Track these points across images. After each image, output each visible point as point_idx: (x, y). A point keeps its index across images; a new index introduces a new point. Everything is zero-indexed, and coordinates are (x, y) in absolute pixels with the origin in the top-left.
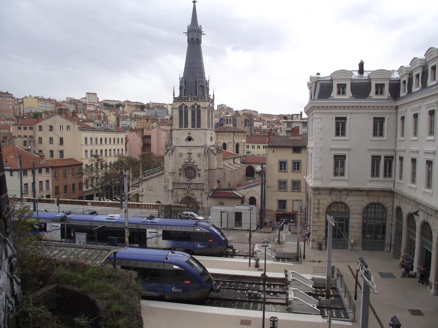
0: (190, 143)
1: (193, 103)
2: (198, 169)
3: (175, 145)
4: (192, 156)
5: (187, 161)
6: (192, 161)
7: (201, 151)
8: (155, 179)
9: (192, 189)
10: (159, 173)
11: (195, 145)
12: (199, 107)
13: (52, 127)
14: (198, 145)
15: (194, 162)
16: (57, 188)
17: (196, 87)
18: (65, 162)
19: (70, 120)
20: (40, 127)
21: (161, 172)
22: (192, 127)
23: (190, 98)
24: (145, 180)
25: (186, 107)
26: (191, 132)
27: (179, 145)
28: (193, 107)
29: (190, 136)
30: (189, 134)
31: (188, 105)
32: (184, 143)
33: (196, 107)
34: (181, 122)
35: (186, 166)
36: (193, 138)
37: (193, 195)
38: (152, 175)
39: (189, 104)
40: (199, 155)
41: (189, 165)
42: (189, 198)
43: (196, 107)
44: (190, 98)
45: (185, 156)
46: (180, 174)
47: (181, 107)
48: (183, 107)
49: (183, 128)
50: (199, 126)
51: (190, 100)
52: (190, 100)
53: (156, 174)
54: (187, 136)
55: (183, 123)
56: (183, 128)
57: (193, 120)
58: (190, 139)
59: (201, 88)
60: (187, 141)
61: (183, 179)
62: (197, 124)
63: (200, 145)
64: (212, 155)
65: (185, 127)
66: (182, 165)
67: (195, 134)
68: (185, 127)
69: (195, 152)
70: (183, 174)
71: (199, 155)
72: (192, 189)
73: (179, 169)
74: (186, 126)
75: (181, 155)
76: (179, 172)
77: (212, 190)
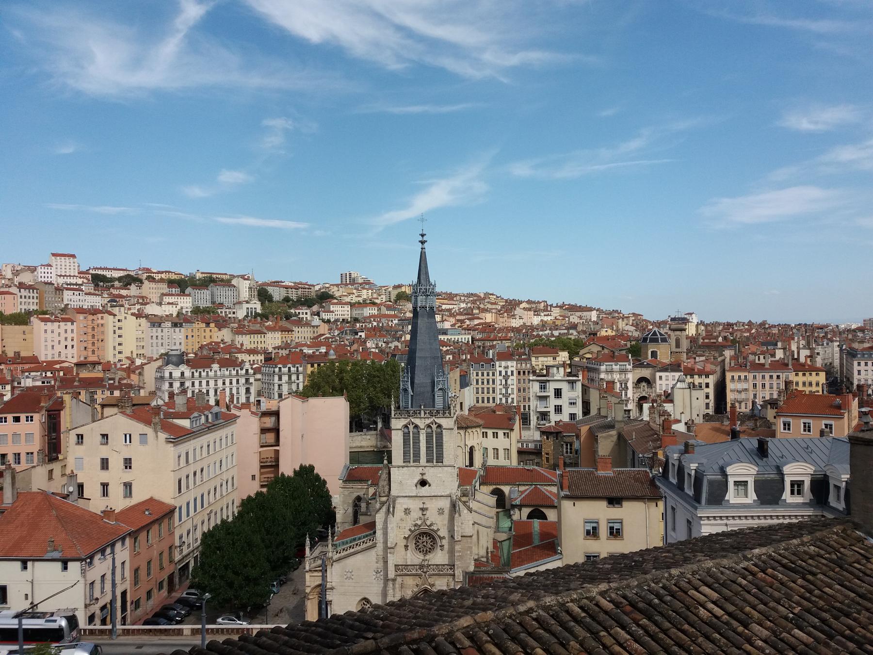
0: (425, 491)
1: (428, 421)
2: (439, 537)
3: (396, 495)
4: (428, 513)
5: (419, 522)
6: (428, 523)
7: (446, 504)
8: (359, 557)
9: (430, 575)
10: (365, 546)
11: (433, 494)
12: (439, 426)
13: (107, 435)
14: (439, 494)
15: (431, 525)
16: (136, 571)
17: (433, 391)
18: (147, 513)
19: (148, 422)
20: (80, 437)
21: (370, 544)
22: (428, 461)
23: (422, 412)
24: (340, 559)
25: (416, 427)
26: (426, 470)
27: (404, 495)
28: (429, 426)
29: (425, 477)
30: (422, 474)
31: (419, 424)
32: (414, 491)
33: (434, 426)
34: (406, 453)
35: (417, 532)
36: (429, 480)
37: (433, 585)
38: (352, 550)
39: (421, 423)
40: (441, 511)
41: (423, 531)
42: (426, 591)
43: (434, 426)
44: (422, 412)
45: (416, 514)
46: (406, 547)
47: (406, 426)
48: (411, 427)
49: (412, 464)
50: (440, 459)
51: (422, 415)
52: (422, 415)
53: (358, 548)
54: (418, 478)
55: (411, 456)
56: (412, 464)
57: (429, 448)
58: (423, 483)
59: (441, 393)
60: (419, 486)
61: (413, 557)
62: (436, 456)
63: (443, 494)
64: (466, 511)
65: (414, 461)
66: (410, 530)
67: (431, 474)
68: (414, 461)
69: (433, 506)
70: (412, 546)
71: (441, 511)
72: (430, 575)
73: (405, 538)
74: (417, 458)
75: (407, 511)
76: (404, 542)
77: (466, 573)
